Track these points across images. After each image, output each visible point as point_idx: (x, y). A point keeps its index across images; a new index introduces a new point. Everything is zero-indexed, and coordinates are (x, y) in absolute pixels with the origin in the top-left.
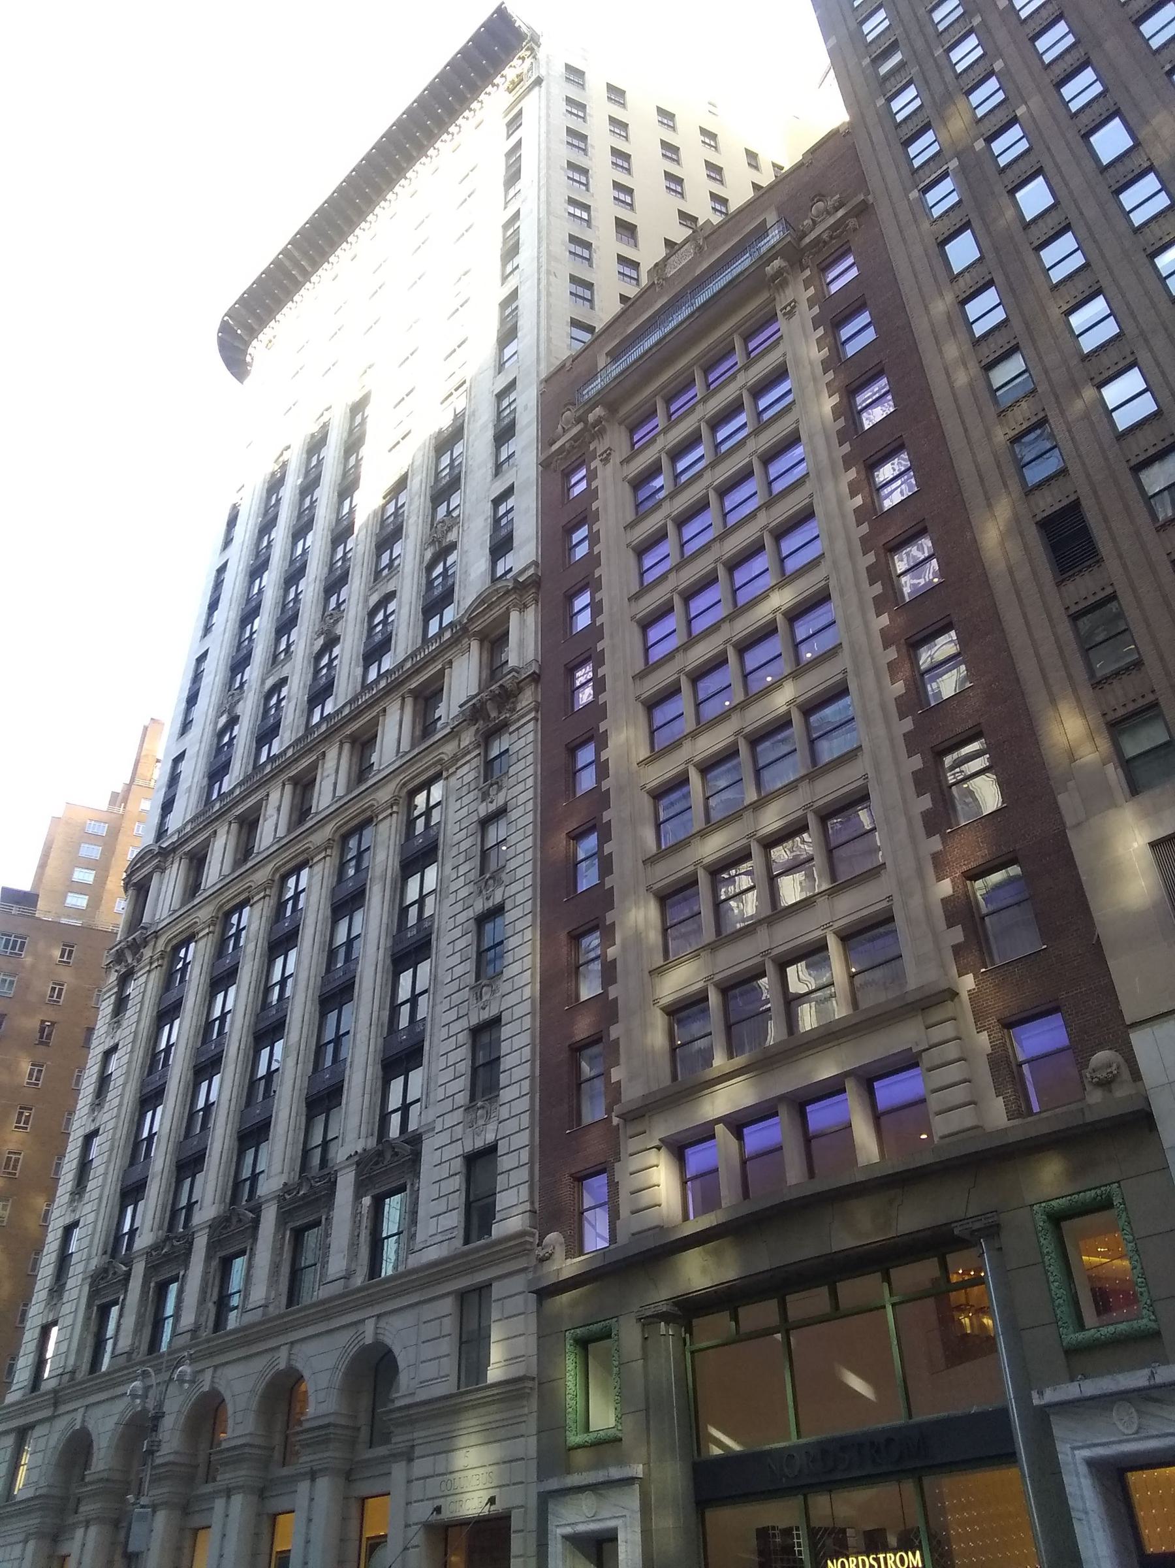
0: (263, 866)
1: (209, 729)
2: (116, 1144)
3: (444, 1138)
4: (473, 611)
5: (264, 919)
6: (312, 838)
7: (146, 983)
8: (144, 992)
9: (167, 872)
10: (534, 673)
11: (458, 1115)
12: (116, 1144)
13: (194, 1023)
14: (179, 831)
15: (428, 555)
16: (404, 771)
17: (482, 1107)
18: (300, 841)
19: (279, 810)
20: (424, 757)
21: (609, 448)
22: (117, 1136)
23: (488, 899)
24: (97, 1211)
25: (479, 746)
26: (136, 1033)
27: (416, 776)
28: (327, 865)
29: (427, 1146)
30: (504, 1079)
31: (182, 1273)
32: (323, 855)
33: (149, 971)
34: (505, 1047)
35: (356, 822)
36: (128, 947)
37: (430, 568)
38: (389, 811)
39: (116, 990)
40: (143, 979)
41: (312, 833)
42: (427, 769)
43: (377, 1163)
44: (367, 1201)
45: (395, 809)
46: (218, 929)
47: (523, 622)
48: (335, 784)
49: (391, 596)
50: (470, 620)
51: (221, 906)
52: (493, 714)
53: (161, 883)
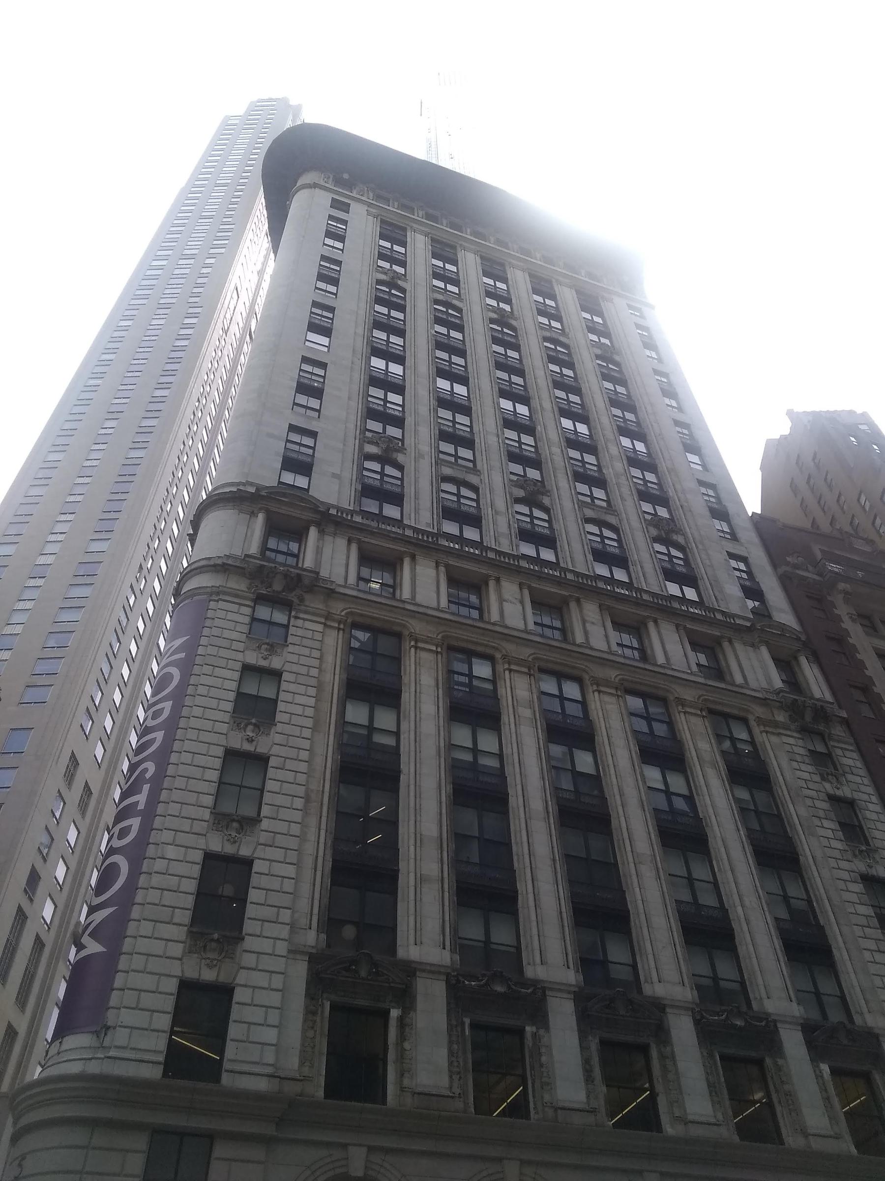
15: (654, 532)
19: (522, 602)
23: (871, 867)
25: (799, 732)
31: (528, 1029)
32: (613, 691)
35: (643, 688)
36: (286, 575)
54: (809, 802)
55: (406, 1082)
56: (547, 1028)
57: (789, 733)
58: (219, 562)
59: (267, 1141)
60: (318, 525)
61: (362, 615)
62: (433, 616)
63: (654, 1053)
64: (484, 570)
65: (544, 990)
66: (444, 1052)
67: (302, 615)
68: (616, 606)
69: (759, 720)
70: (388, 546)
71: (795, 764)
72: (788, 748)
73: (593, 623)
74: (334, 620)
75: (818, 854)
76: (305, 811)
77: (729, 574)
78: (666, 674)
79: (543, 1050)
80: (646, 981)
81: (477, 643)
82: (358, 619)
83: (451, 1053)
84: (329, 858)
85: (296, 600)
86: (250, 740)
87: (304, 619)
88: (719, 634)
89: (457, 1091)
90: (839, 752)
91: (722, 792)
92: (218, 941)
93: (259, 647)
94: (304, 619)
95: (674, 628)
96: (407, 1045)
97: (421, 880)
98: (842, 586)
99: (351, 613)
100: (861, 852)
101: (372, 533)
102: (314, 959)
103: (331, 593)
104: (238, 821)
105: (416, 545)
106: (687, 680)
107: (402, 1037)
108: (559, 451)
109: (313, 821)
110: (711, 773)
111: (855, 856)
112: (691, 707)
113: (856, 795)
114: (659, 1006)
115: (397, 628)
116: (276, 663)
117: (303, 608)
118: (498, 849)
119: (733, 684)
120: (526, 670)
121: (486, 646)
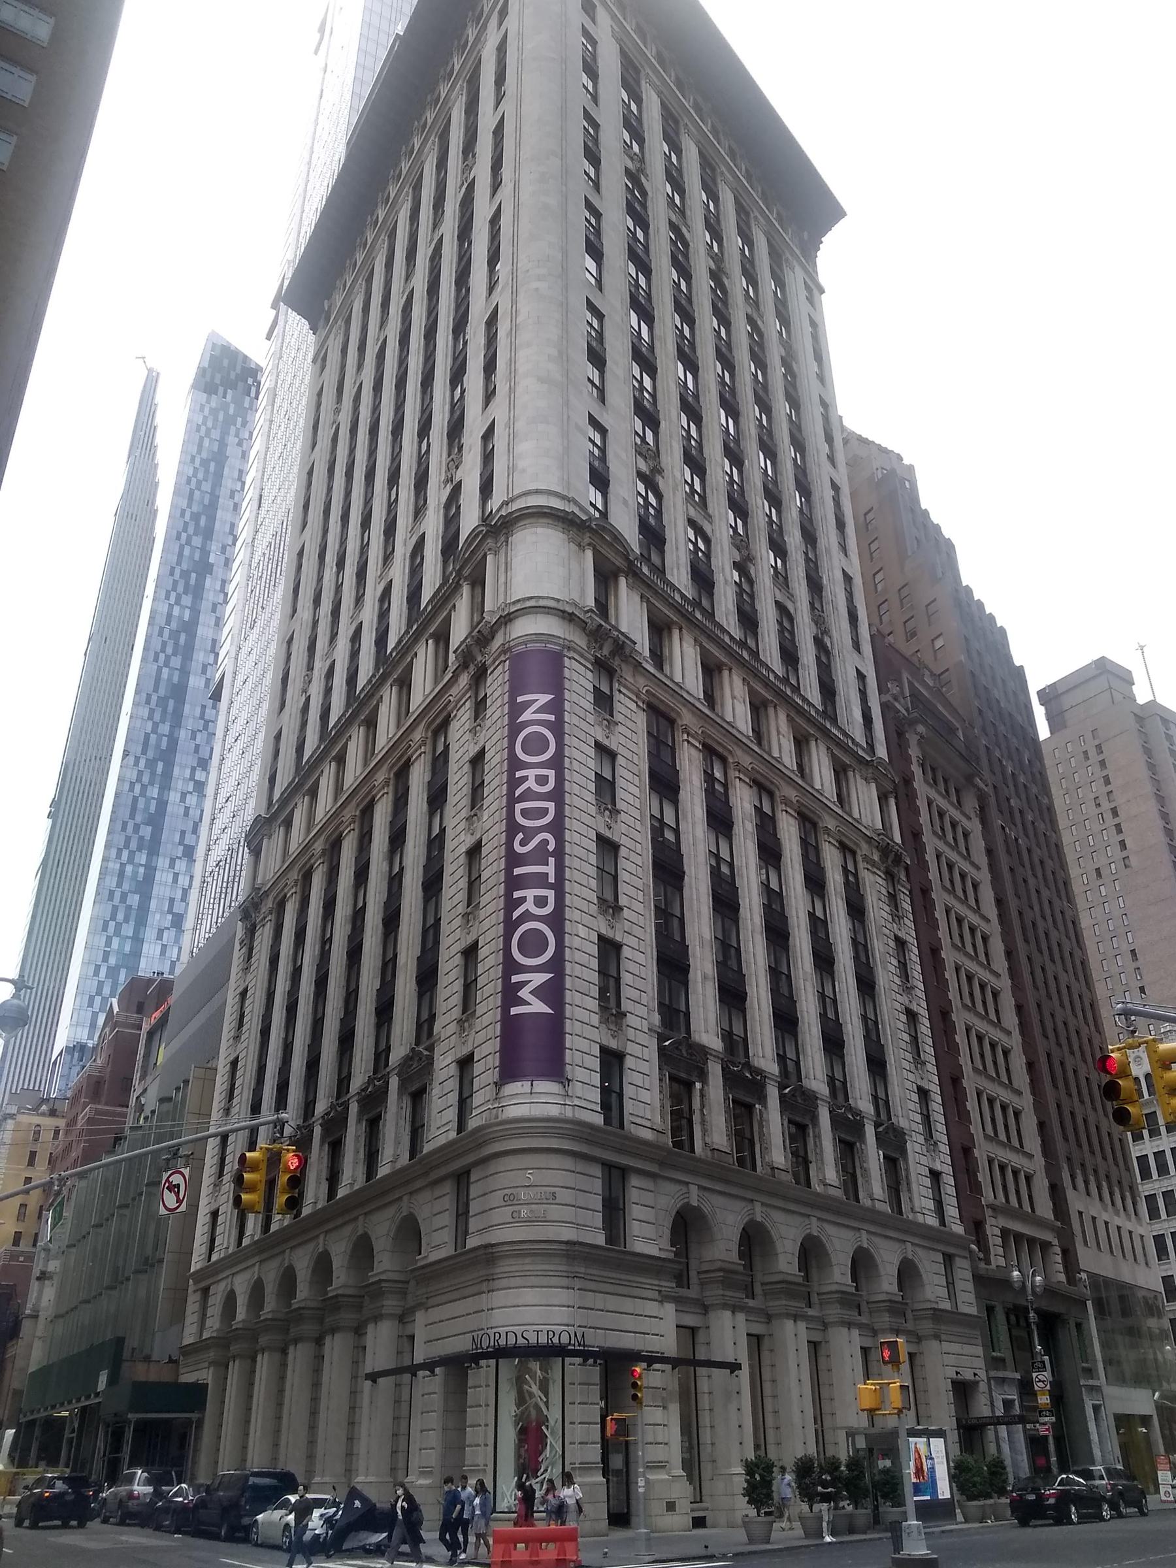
36: (616, 640)
44: (881, 1152)
55: (708, 1140)
56: (765, 1105)
58: (569, 609)
59: (653, 1176)
64: (723, 658)
69: (866, 859)
81: (719, 743)
97: (705, 977)
101: (656, 593)
102: (661, 1038)
105: (683, 615)
107: (703, 1106)
110: (839, 901)
115: (673, 715)
119: (850, 815)
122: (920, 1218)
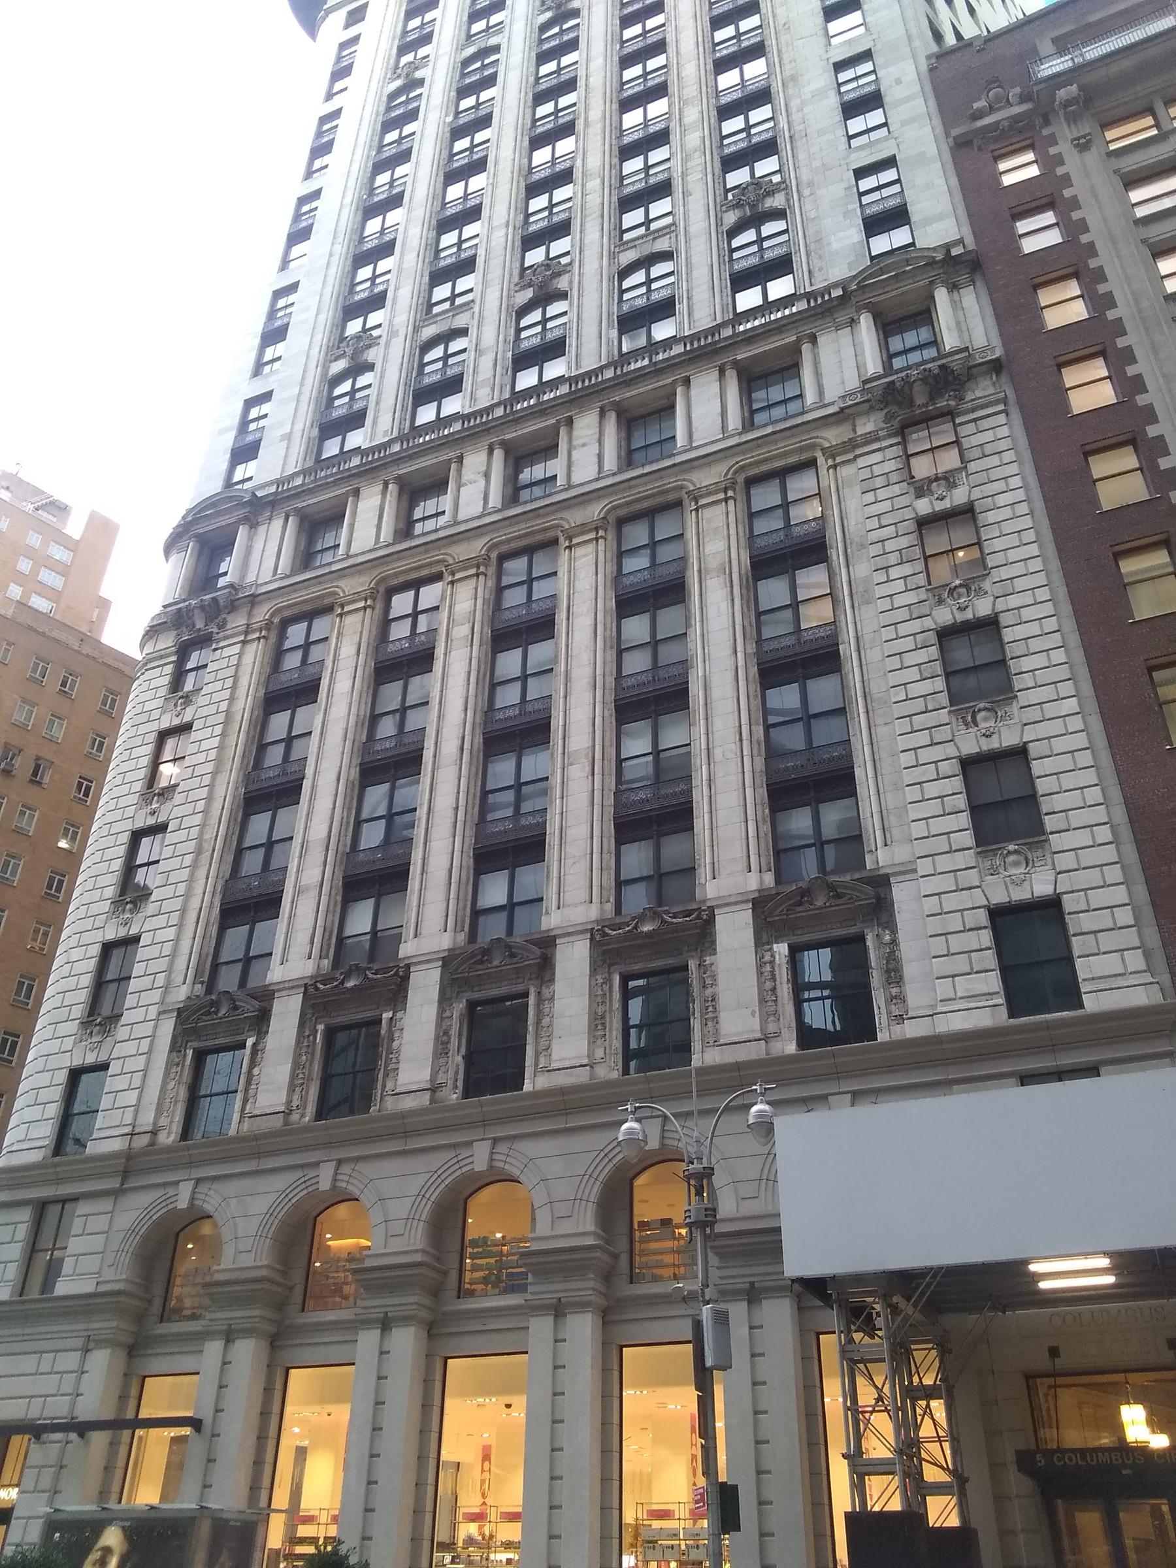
0: (468, 539)
1: (313, 375)
2: (208, 847)
3: (947, 883)
4: (865, 279)
5: (480, 602)
6: (565, 514)
7: (240, 655)
8: (238, 665)
9: (262, 529)
10: (998, 360)
11: (968, 858)
12: (208, 847)
13: (354, 710)
14: (279, 482)
15: (731, 218)
16: (743, 453)
17: (1016, 852)
18: (539, 516)
19: (487, 475)
20: (783, 439)
21: (1089, 134)
22: (209, 834)
24: (180, 926)
25: (895, 435)
26: (228, 713)
27: (766, 460)
28: (601, 547)
29: (901, 894)
30: (1050, 823)
31: (386, 1016)
32: (593, 535)
33: (244, 642)
34: (1042, 786)
35: (645, 504)
36: (202, 608)
37: (733, 233)
38: (722, 496)
39: (174, 658)
40: (236, 649)
41: (564, 509)
42: (786, 454)
43: (800, 904)
45: (730, 493)
46: (379, 605)
47: (956, 305)
48: (600, 457)
49: (667, 256)
50: (862, 288)
51: (383, 579)
52: (920, 400)
53: (250, 539)
54: (874, 550)
57: (876, 446)
60: (246, 520)
61: (289, 606)
62: (362, 563)
63: (532, 1000)
65: (408, 966)
66: (288, 1067)
67: (222, 644)
68: (628, 395)
70: (332, 495)
71: (870, 497)
72: (865, 474)
73: (584, 445)
74: (254, 631)
75: (867, 630)
76: (194, 866)
77: (846, 214)
78: (674, 465)
79: (396, 1035)
80: (547, 913)
82: (287, 613)
83: (296, 1065)
84: (217, 904)
85: (215, 630)
86: (153, 813)
87: (222, 648)
88: (794, 338)
89: (295, 1104)
90: (971, 428)
91: (724, 606)
92: (100, 1024)
93: (176, 705)
94: (222, 648)
95: (715, 374)
96: (256, 1071)
98: (1062, 94)
99: (279, 610)
100: (952, 591)
103: (254, 600)
104: (131, 902)
106: (707, 455)
107: (253, 1063)
108: (598, 181)
109: (201, 873)
111: (940, 601)
112: (710, 494)
113: (976, 494)
114: (547, 944)
116: (187, 718)
117: (221, 635)
118: (398, 822)
120: (473, 571)
121: (431, 564)
122: (911, 1030)
